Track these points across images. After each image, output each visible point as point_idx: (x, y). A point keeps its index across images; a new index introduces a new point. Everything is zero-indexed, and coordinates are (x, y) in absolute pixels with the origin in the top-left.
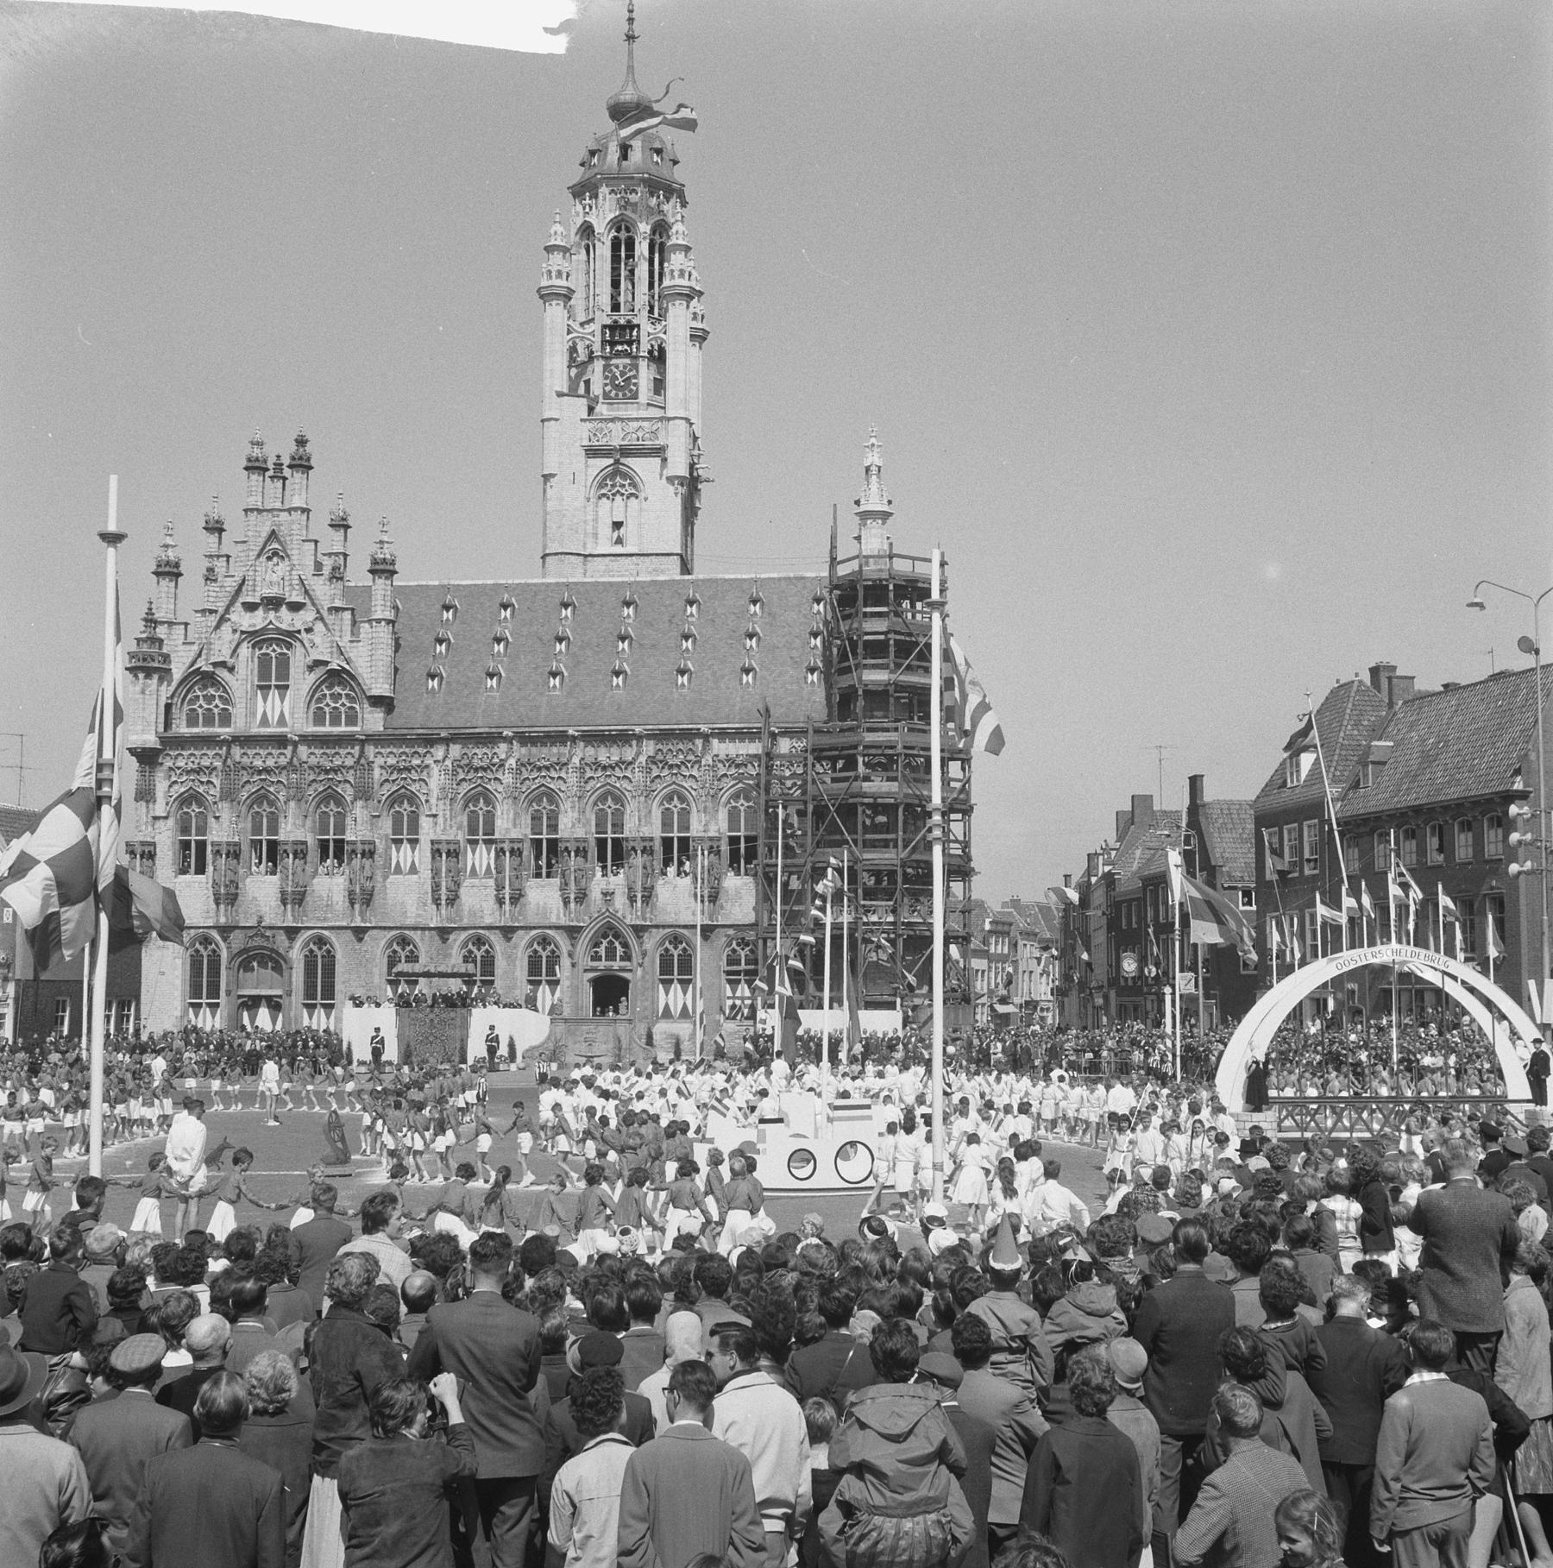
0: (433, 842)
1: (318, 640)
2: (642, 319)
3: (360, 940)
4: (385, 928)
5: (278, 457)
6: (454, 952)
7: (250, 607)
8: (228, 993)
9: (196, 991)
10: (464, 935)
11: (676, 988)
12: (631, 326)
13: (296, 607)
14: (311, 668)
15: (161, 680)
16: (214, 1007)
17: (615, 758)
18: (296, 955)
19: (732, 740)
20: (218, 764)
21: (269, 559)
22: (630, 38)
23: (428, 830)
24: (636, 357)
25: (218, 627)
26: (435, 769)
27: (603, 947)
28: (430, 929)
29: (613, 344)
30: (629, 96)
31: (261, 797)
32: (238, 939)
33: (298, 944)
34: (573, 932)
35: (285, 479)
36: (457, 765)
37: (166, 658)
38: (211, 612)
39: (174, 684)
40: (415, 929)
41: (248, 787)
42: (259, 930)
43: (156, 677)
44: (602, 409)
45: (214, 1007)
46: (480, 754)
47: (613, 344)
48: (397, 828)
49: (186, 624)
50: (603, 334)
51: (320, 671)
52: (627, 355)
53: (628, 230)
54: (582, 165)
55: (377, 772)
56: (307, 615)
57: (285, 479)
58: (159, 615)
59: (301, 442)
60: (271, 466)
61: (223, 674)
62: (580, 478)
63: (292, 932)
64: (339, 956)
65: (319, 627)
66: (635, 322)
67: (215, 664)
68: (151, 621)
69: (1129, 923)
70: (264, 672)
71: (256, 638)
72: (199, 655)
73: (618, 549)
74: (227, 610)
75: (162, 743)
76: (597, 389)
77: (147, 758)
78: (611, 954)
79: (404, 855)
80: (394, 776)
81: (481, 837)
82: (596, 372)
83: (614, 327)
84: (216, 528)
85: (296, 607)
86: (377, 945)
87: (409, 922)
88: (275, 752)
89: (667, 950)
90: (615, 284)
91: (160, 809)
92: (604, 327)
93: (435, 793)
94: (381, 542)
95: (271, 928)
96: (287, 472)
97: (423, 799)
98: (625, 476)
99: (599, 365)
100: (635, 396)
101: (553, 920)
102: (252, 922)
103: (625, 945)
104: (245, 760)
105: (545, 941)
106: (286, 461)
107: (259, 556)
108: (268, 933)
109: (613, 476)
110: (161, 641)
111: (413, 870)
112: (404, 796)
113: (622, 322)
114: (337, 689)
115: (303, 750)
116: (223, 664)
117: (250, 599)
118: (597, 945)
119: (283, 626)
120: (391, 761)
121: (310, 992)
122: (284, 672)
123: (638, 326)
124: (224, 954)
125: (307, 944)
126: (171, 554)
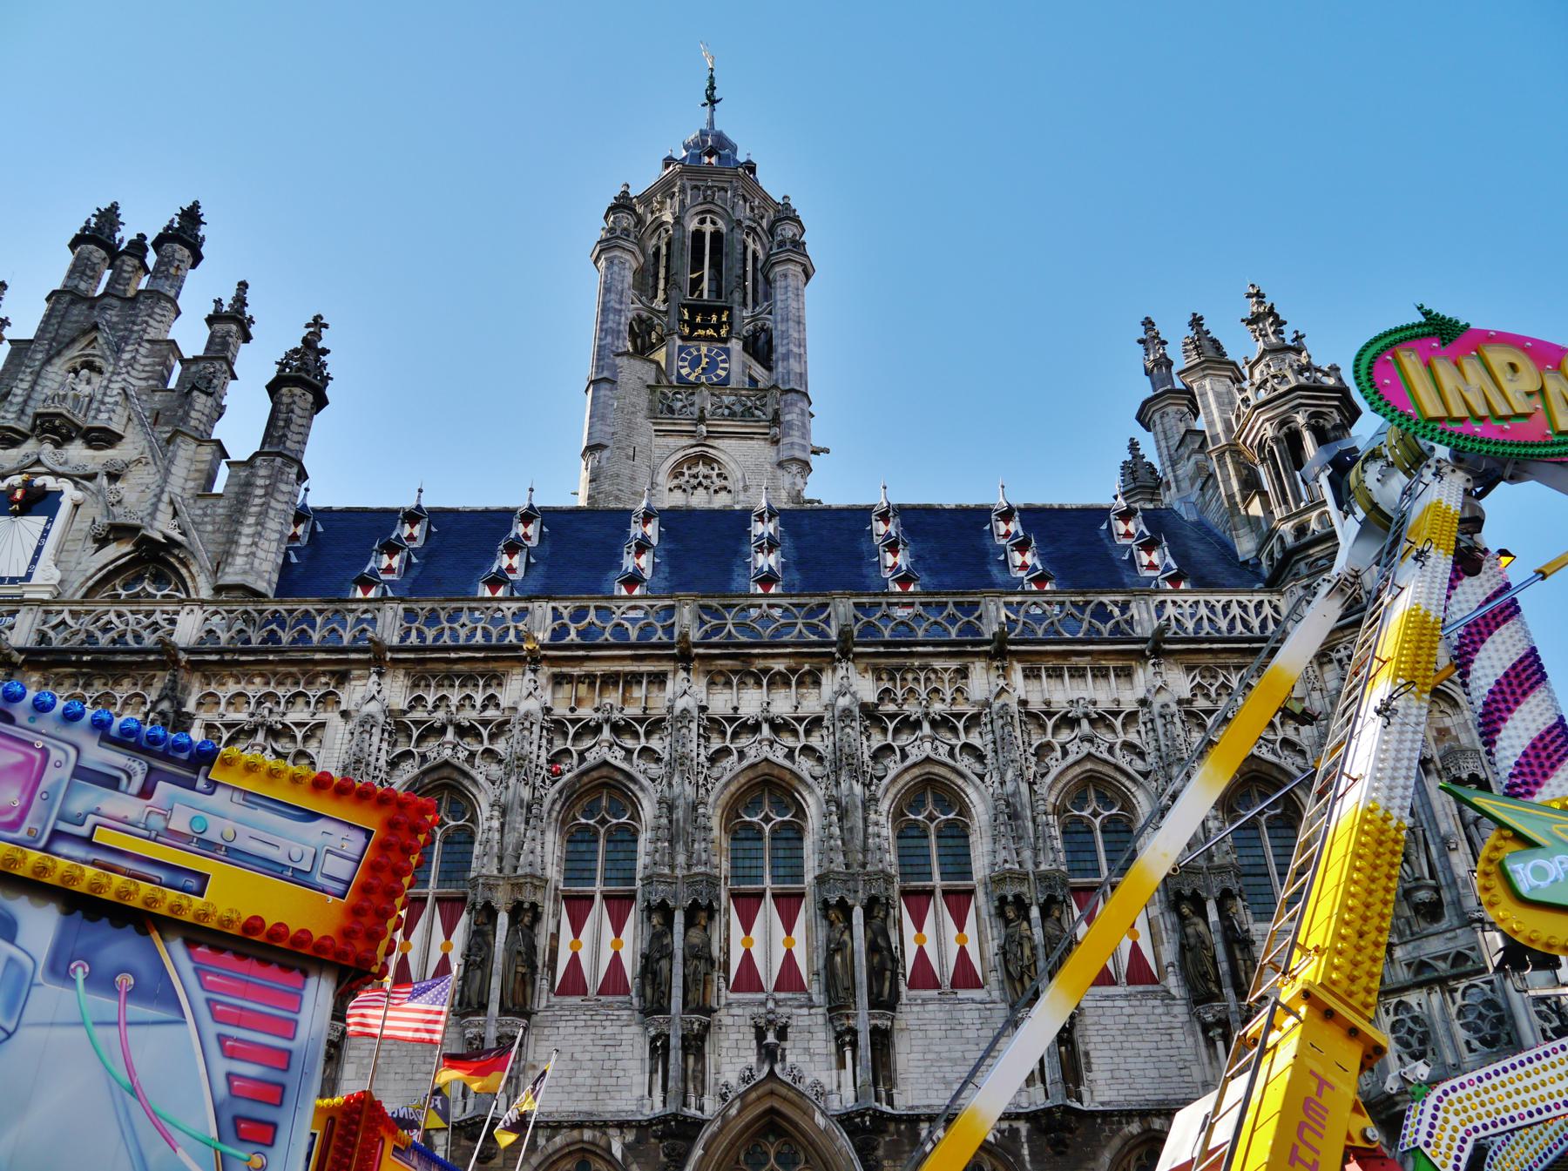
13: (103, 438)
14: (102, 542)
19: (1055, 673)
24: (725, 340)
29: (694, 327)
34: (677, 1131)
36: (398, 726)
46: (459, 702)
47: (694, 327)
51: (116, 551)
53: (713, 223)
59: (192, 216)
92: (684, 306)
96: (151, 259)
98: (709, 461)
107: (48, 361)
123: (730, 309)
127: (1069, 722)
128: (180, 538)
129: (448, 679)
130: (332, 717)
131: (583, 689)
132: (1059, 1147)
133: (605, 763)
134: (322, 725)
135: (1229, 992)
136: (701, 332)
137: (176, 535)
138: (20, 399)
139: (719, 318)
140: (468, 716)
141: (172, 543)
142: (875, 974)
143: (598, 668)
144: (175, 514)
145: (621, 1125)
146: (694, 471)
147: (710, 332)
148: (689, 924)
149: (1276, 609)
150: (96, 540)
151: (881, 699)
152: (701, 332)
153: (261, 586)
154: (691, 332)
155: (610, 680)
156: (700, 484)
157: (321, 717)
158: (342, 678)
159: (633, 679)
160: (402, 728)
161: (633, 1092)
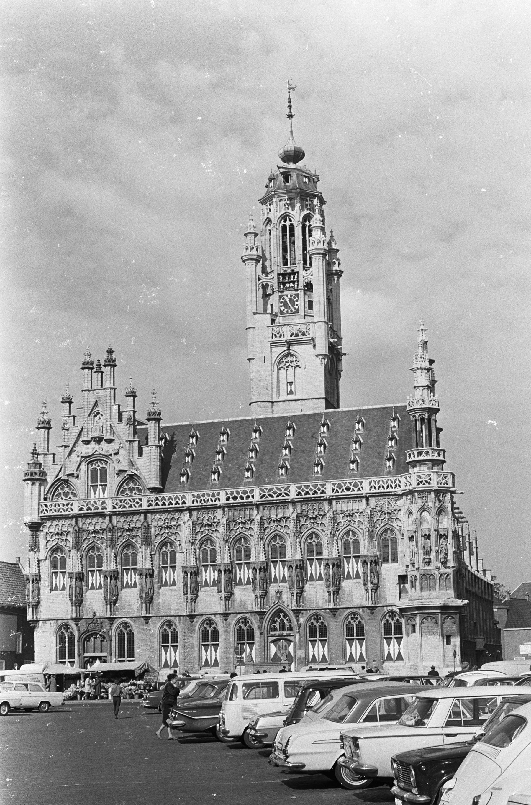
0: (183, 567)
1: (121, 459)
2: (299, 268)
3: (147, 623)
5: (99, 361)
6: (197, 628)
7: (87, 443)
8: (79, 655)
11: (318, 644)
12: (293, 273)
13: (109, 441)
15: (40, 485)
16: (72, 663)
17: (280, 515)
20: (71, 529)
21: (95, 416)
22: (290, 116)
25: (69, 455)
26: (184, 527)
27: (278, 623)
30: (290, 147)
31: (128, 545)
33: (114, 627)
34: (261, 614)
35: (102, 373)
37: (44, 474)
38: (66, 447)
39: (48, 487)
41: (121, 539)
42: (93, 619)
43: (37, 484)
44: (280, 320)
45: (72, 663)
47: (284, 284)
49: (54, 454)
50: (279, 278)
53: (290, 220)
54: (266, 187)
55: (153, 530)
56: (114, 446)
57: (102, 373)
58: (39, 451)
59: (110, 352)
60: (95, 366)
61: (72, 480)
62: (268, 358)
63: (112, 620)
64: (135, 633)
66: (296, 270)
67: (68, 475)
68: (35, 454)
69: (476, 603)
70: (94, 479)
71: (90, 459)
72: (60, 471)
73: (291, 397)
74: (74, 446)
75: (42, 519)
76: (276, 310)
77: (35, 527)
78: (282, 627)
79: (168, 576)
80: (162, 532)
81: (209, 563)
82: (274, 299)
83: (284, 275)
84: (69, 401)
85: (109, 441)
87: (172, 613)
88: (100, 520)
89: (240, 627)
90: (285, 250)
91: (42, 555)
92: (279, 275)
93: (184, 539)
94: (153, 403)
96: (103, 369)
97: (178, 543)
98: (292, 355)
99: (276, 295)
100: (297, 311)
101: (250, 609)
102: (90, 616)
103: (289, 621)
104: (85, 527)
105: (245, 621)
106: (103, 363)
107: (89, 415)
109: (286, 356)
110: (40, 465)
111: (174, 584)
112: (168, 542)
113: (289, 271)
114: (132, 485)
116: (72, 475)
117: (85, 439)
118: (274, 622)
119: (103, 453)
122: (104, 479)
123: (298, 273)
124: (76, 634)
126: (46, 417)
128: (136, 472)
132: (334, 615)
133: (241, 532)
134: (180, 525)
135: (369, 583)
136: (287, 285)
138: (86, 430)
139: (294, 278)
142: (298, 581)
146: (286, 360)
147: (291, 284)
148: (260, 571)
149: (400, 482)
150: (117, 474)
151: (302, 512)
152: (287, 285)
154: (284, 286)
156: (289, 365)
157: (179, 523)
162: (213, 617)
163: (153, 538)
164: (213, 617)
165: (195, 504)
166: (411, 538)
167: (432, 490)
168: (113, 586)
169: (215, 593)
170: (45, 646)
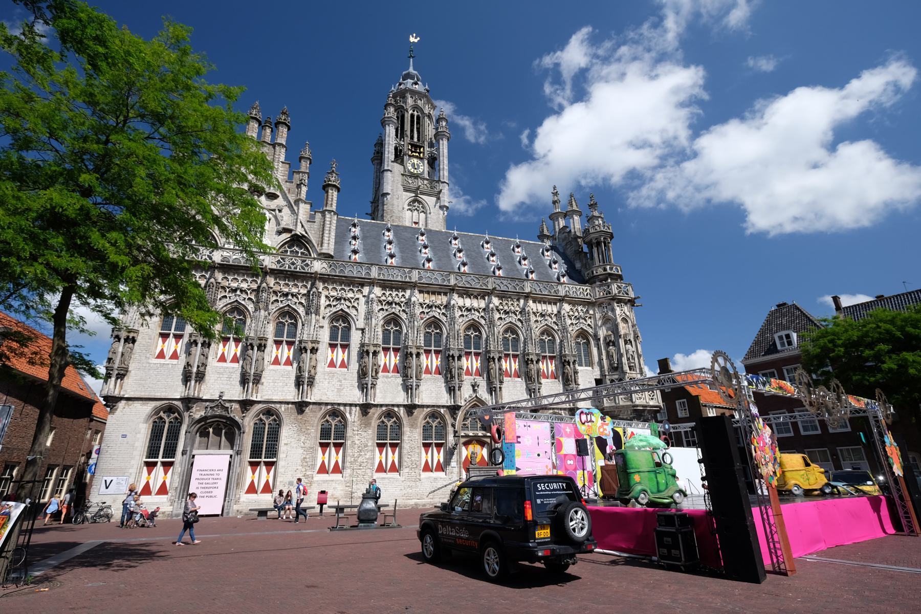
4: (320, 404)
9: (153, 451)
10: (379, 411)
14: (279, 233)
18: (248, 422)
19: (540, 302)
23: (355, 338)
28: (356, 405)
32: (198, 412)
40: (345, 405)
42: (220, 403)
48: (333, 336)
51: (286, 236)
52: (417, 157)
55: (323, 299)
65: (286, 211)
80: (334, 303)
86: (314, 418)
88: (249, 280)
95: (230, 401)
98: (419, 202)
108: (227, 405)
114: (296, 248)
115: (271, 281)
120: (334, 293)
121: (256, 451)
125: (258, 415)
127: (542, 315)
129: (391, 289)
130: (359, 296)
131: (426, 295)
134: (358, 299)
137: (304, 233)
140: (397, 300)
141: (303, 236)
143: (430, 290)
144: (302, 226)
145: (443, 407)
153: (332, 253)
155: (434, 293)
157: (357, 296)
158: (362, 285)
159: (439, 293)
160: (380, 301)
161: (444, 399)
162: (396, 409)
163: (322, 308)
164: (396, 409)
165: (382, 277)
166: (608, 344)
167: (629, 301)
168: (260, 358)
169: (400, 380)
170: (124, 436)
